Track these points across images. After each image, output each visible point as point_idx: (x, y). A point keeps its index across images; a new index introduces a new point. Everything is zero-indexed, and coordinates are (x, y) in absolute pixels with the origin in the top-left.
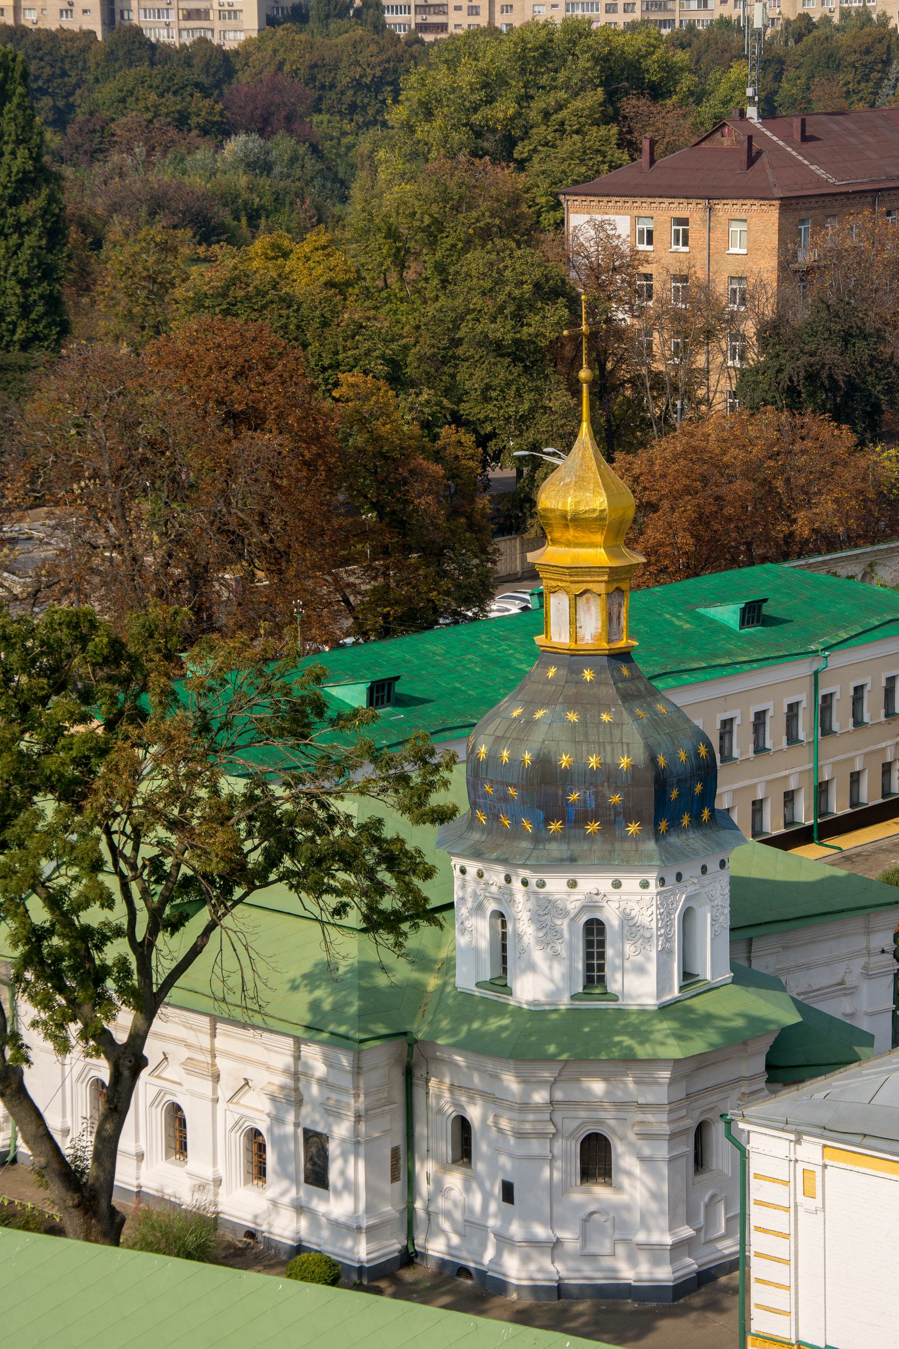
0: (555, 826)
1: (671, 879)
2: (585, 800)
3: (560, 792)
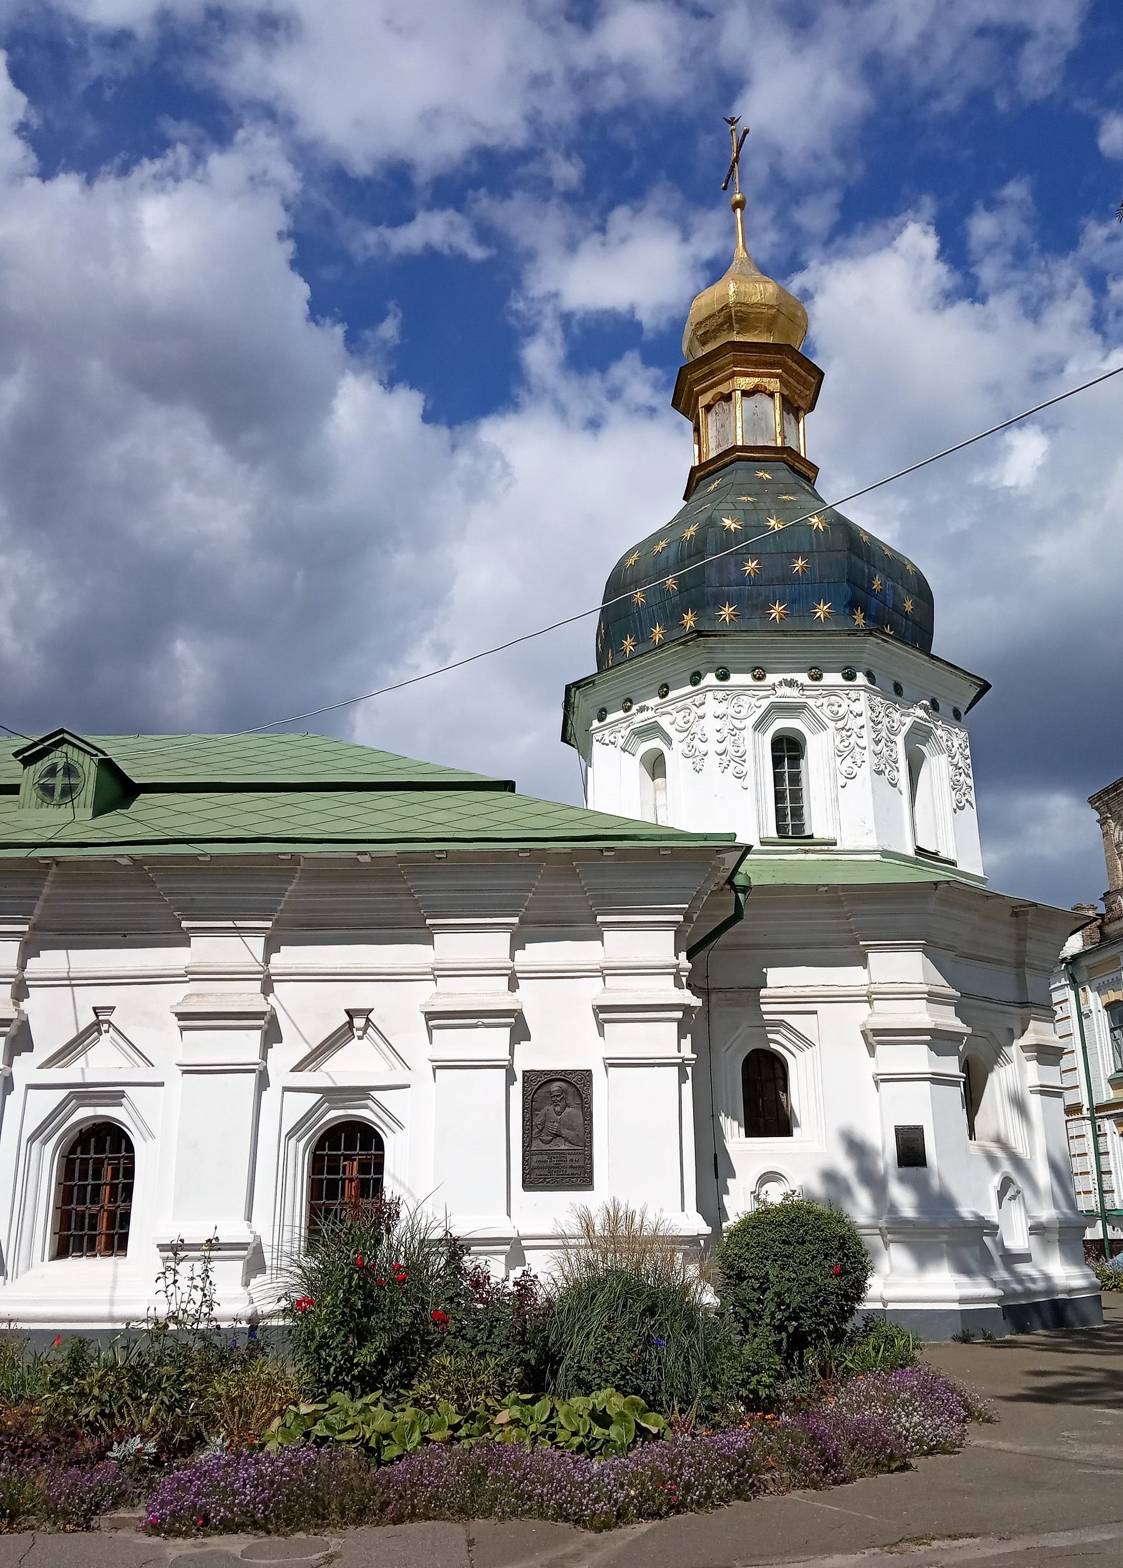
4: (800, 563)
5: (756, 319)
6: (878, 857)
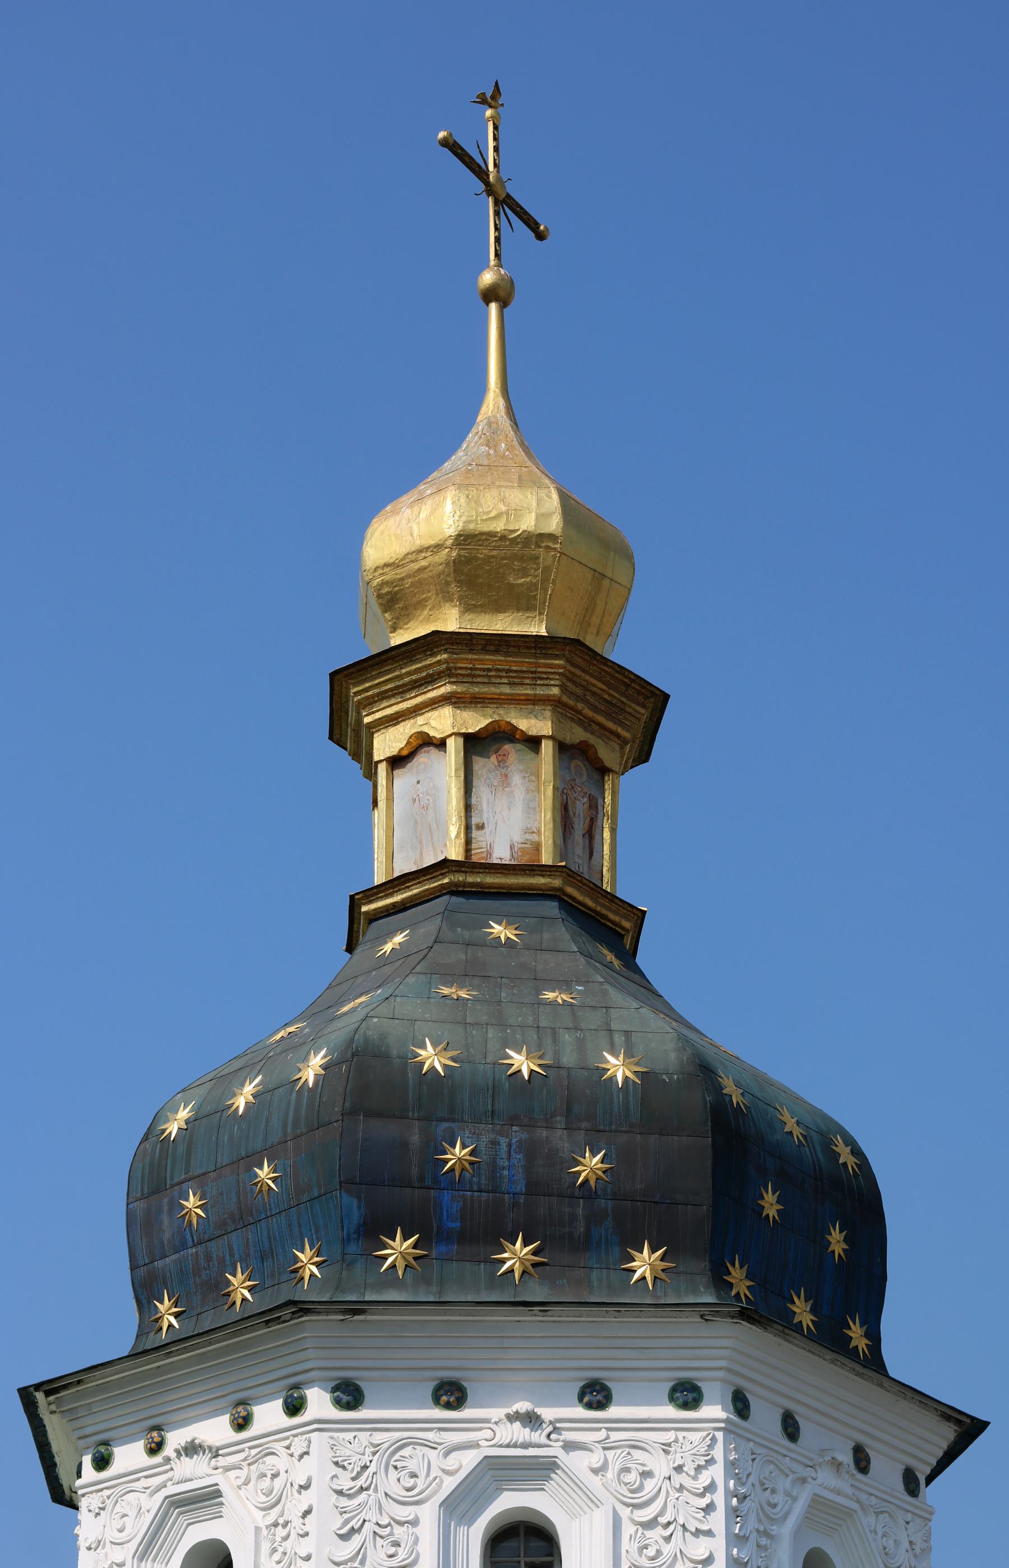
0: (398, 1249)
1: (766, 1418)
2: (494, 1168)
3: (415, 1138)
4: (264, 1173)
5: (420, 583)
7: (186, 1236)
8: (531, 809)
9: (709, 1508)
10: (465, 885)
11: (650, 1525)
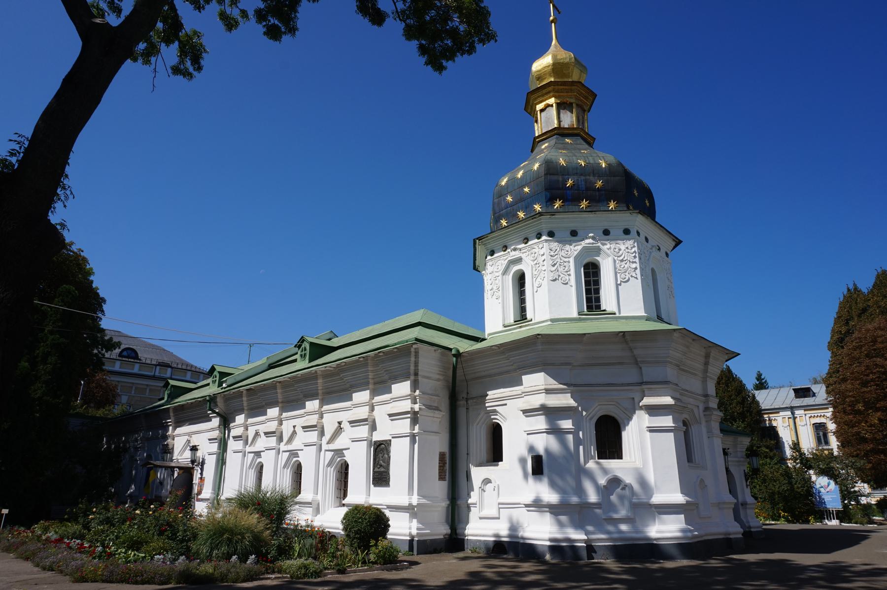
0: (557, 205)
3: (561, 179)
4: (526, 190)
6: (549, 323)
7: (508, 205)
8: (572, 117)
9: (635, 257)
10: (560, 132)
11: (622, 261)
